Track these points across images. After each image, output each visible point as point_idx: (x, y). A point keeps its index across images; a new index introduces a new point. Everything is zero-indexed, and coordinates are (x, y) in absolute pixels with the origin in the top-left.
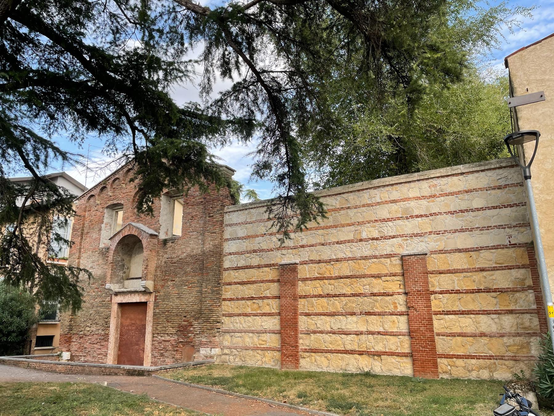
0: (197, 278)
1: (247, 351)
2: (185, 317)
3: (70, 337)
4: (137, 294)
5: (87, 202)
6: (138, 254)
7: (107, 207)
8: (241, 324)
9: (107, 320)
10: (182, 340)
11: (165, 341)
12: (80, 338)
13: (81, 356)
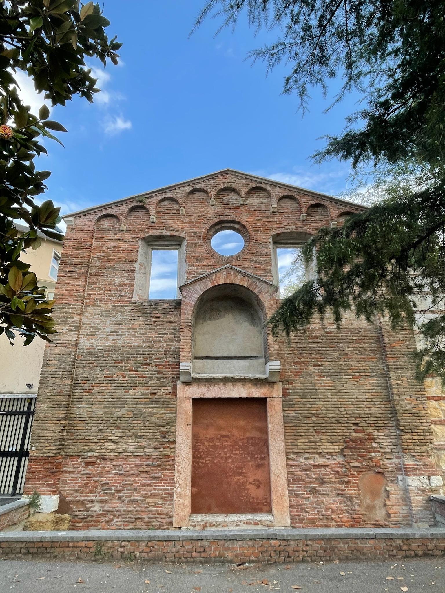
0: (370, 363)
2: (356, 424)
4: (240, 384)
5: (96, 224)
6: (210, 319)
7: (144, 239)
9: (164, 429)
10: (357, 464)
11: (315, 466)
12: (88, 464)
13: (92, 501)
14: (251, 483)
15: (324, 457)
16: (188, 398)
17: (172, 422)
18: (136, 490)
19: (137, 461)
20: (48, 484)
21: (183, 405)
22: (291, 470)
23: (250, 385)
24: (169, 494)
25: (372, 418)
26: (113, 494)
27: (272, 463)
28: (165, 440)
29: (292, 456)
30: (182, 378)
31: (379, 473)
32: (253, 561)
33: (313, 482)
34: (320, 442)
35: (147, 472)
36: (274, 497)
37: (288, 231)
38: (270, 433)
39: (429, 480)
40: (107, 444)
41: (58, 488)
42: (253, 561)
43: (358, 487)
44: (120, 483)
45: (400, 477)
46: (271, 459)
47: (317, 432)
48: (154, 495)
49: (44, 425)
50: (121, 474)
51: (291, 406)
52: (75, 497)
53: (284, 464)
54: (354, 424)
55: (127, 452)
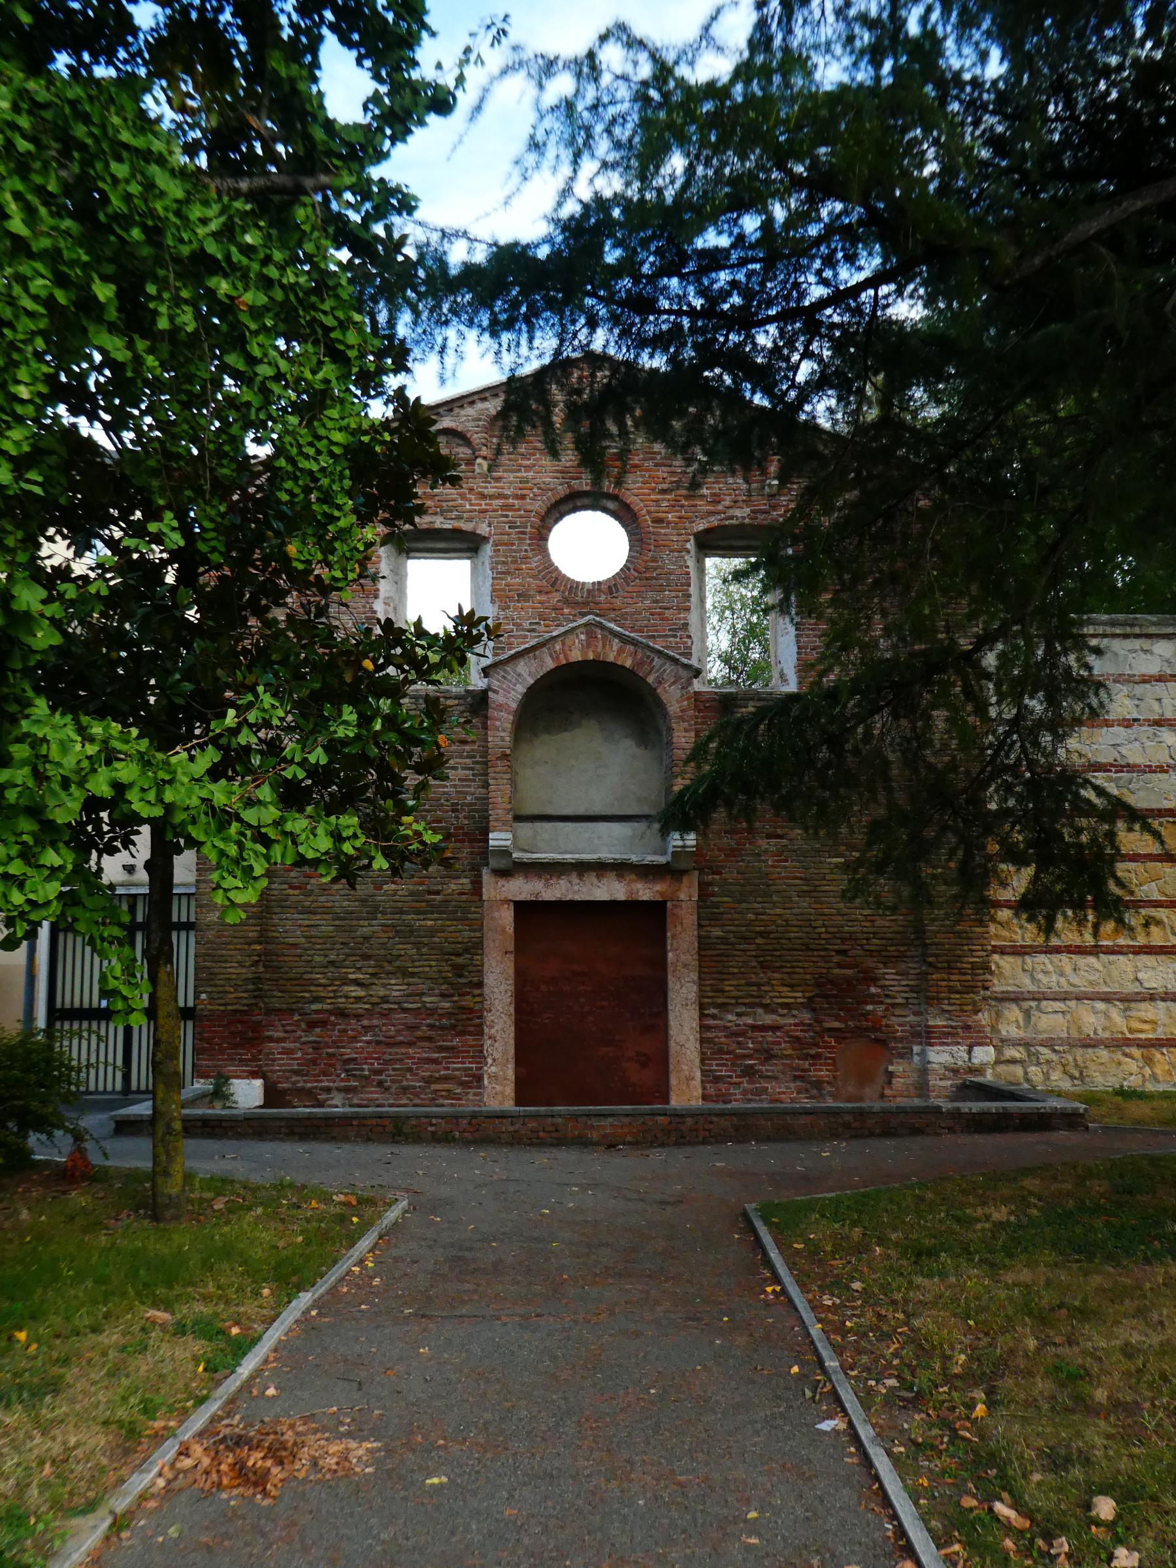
1: (1090, 1050)
3: (257, 1027)
4: (612, 875)
6: (548, 730)
8: (1062, 974)
9: (460, 960)
10: (836, 1025)
11: (755, 1028)
12: (312, 1025)
13: (328, 1090)
14: (630, 1059)
15: (774, 1012)
16: (507, 901)
17: (476, 947)
18: (410, 1070)
19: (411, 1020)
20: (241, 1060)
21: (496, 915)
22: (709, 1035)
23: (633, 876)
24: (474, 1076)
25: (875, 941)
26: (366, 1078)
27: (673, 1022)
28: (462, 981)
29: (713, 1011)
30: (493, 862)
31: (877, 1040)
32: (630, 1143)
33: (750, 1057)
34: (769, 984)
35: (430, 1039)
36: (673, 1081)
37: (734, 522)
38: (670, 969)
39: (970, 1052)
40: (346, 988)
41: (260, 1066)
42: (630, 1143)
43: (834, 1064)
44: (378, 1059)
45: (916, 1049)
46: (671, 1016)
47: (764, 966)
48: (446, 1079)
49: (220, 952)
50: (378, 1043)
51: (715, 919)
52: (294, 1083)
53: (695, 1024)
54: (839, 952)
55: (387, 1002)
